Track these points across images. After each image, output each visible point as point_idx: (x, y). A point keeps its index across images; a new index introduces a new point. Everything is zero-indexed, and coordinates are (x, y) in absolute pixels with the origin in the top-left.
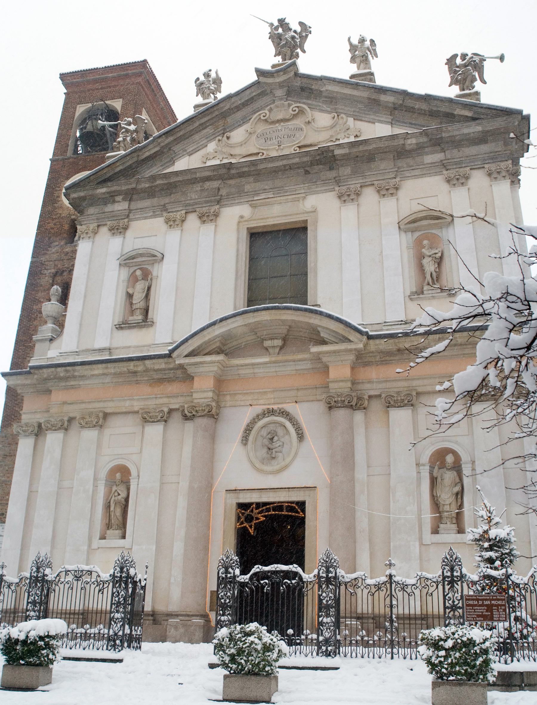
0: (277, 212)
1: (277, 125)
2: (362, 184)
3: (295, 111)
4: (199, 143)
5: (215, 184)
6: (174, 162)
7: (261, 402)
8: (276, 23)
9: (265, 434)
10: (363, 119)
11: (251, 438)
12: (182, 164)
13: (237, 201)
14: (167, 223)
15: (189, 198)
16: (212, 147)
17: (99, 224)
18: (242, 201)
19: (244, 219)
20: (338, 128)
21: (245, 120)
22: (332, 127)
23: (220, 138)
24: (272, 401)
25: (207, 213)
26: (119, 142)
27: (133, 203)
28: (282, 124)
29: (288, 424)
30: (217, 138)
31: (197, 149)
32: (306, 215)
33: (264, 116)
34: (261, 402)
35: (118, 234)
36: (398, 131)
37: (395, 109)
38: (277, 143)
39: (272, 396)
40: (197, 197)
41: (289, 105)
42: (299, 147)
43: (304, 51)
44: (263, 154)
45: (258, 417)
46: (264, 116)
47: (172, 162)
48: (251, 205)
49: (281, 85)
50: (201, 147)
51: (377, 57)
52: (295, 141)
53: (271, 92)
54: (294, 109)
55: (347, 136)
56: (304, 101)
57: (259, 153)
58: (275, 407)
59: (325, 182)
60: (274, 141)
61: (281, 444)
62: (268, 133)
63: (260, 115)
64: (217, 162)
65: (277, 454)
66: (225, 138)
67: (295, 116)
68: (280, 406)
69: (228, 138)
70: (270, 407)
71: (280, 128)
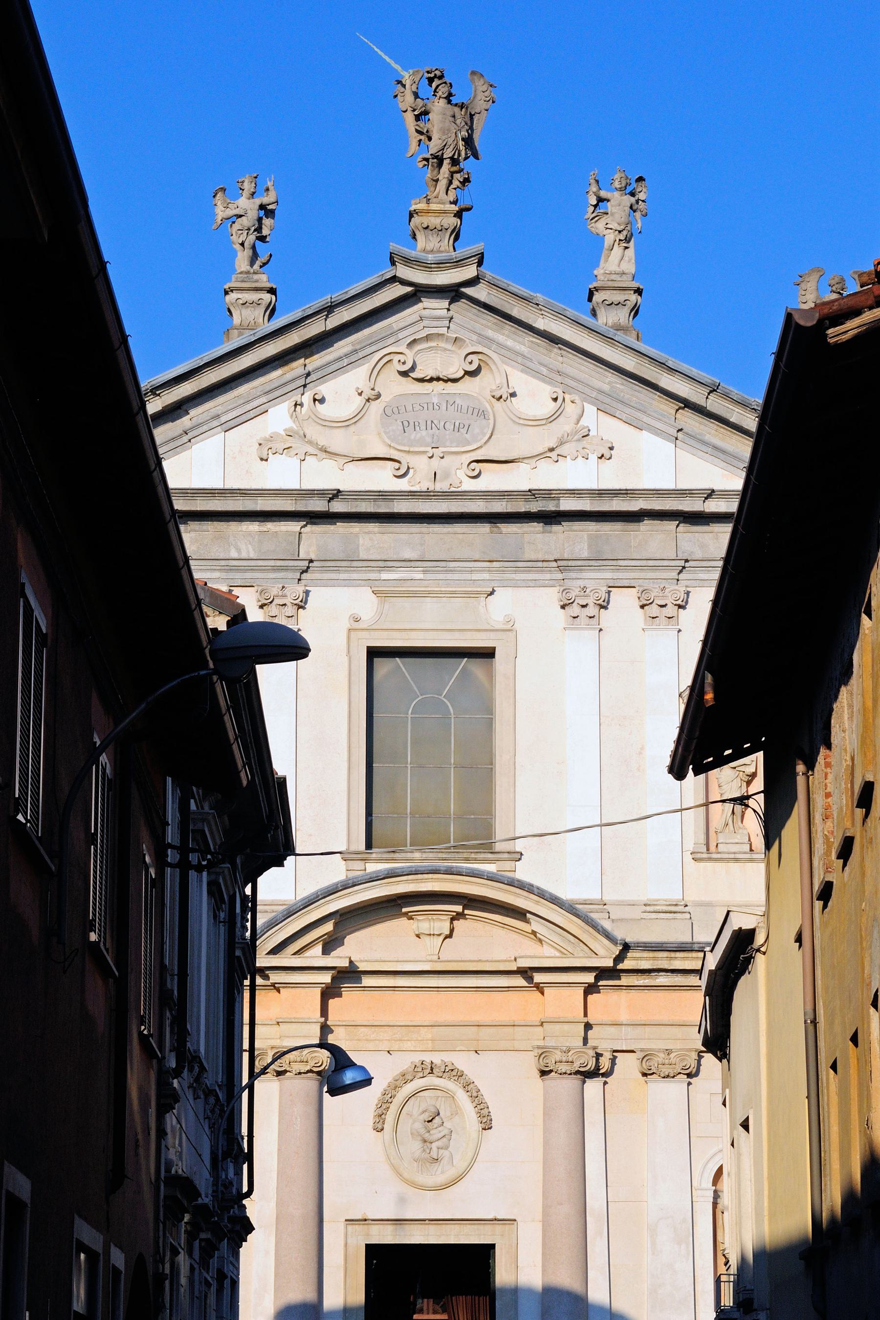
5: (294, 526)
7: (408, 1045)
9: (416, 1113)
11: (390, 1118)
13: (343, 576)
15: (234, 554)
16: (279, 418)
18: (355, 576)
20: (564, 426)
22: (552, 419)
24: (430, 1046)
29: (462, 1096)
31: (244, 418)
32: (492, 635)
34: (408, 1045)
38: (429, 440)
39: (429, 1036)
40: (252, 556)
45: (404, 1078)
52: (469, 443)
58: (437, 1059)
59: (538, 564)
60: (424, 433)
61: (446, 1132)
62: (409, 408)
65: (441, 1152)
66: (307, 399)
68: (448, 1057)
70: (428, 1058)
71: (435, 400)
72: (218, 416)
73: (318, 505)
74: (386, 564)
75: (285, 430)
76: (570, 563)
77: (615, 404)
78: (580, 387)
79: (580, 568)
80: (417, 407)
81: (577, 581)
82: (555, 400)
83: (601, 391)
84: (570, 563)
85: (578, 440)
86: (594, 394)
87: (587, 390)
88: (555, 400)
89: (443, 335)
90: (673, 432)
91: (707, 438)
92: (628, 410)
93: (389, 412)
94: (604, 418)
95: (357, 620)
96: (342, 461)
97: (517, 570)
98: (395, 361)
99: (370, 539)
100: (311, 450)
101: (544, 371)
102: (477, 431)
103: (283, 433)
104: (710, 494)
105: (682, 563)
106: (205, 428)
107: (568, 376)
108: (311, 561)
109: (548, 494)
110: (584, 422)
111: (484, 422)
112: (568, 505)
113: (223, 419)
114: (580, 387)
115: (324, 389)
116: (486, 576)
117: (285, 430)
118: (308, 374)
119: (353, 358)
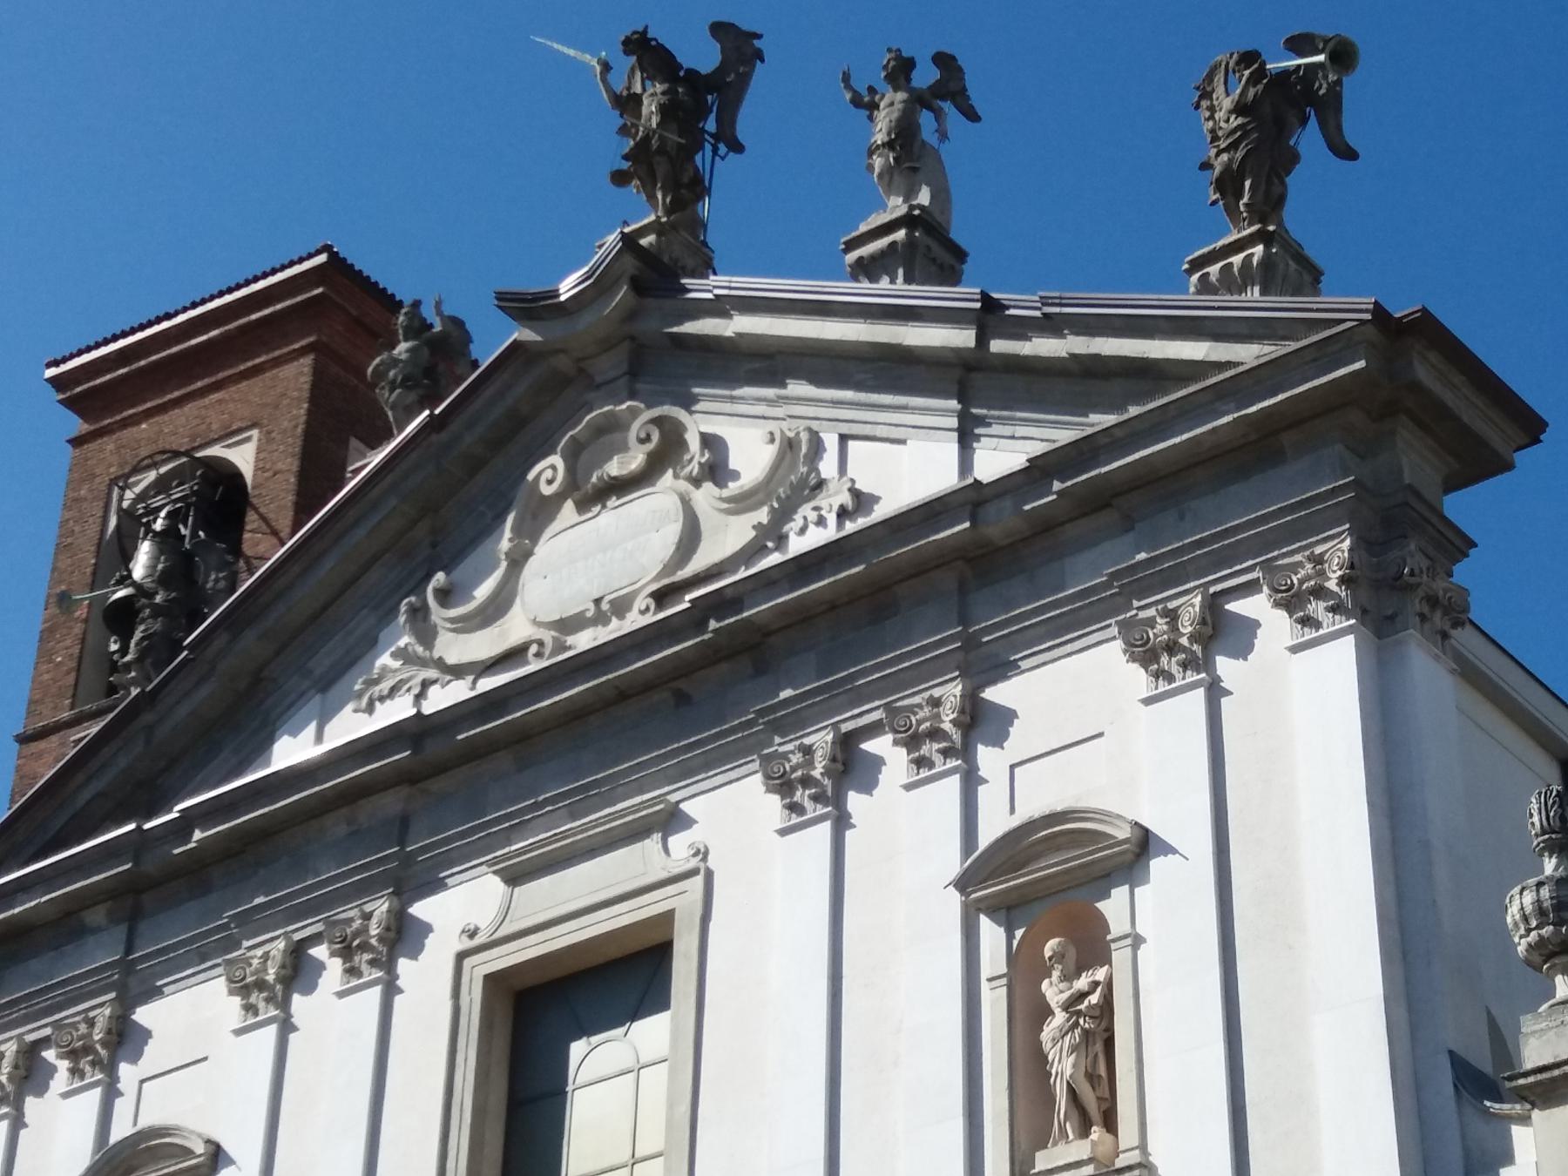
0: (578, 901)
5: (390, 803)
10: (880, 431)
19: (480, 940)
25: (356, 934)
30: (403, 608)
49: (607, 345)
54: (643, 435)
95: (472, 934)
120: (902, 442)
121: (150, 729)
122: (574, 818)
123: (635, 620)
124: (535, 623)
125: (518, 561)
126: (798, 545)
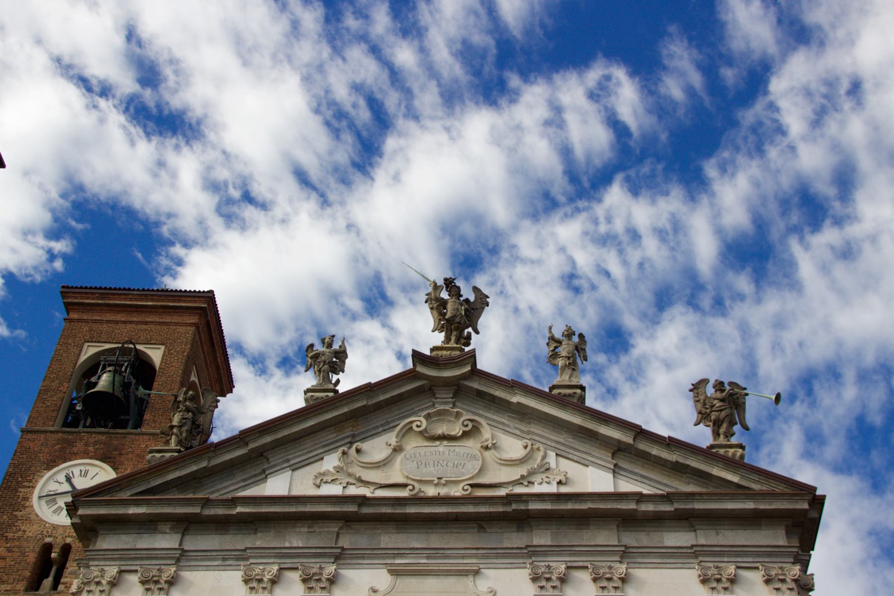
1: (438, 443)
2: (569, 564)
3: (467, 426)
4: (310, 452)
6: (266, 477)
8: (441, 282)
10: (570, 456)
12: (277, 485)
13: (366, 562)
14: (246, 582)
15: (287, 545)
16: (331, 462)
17: (123, 568)
18: (376, 561)
21: (387, 428)
22: (522, 461)
23: (345, 448)
25: (314, 574)
26: (172, 427)
27: (187, 538)
28: (445, 443)
30: (340, 450)
31: (307, 462)
33: (418, 426)
35: (157, 592)
36: (627, 486)
37: (619, 450)
40: (301, 545)
41: (458, 415)
42: (472, 486)
43: (477, 332)
44: (414, 488)
46: (418, 426)
47: (263, 476)
48: (390, 571)
50: (312, 460)
51: (586, 360)
52: (464, 475)
53: (430, 389)
54: (465, 423)
55: (547, 480)
56: (481, 412)
57: (404, 486)
60: (432, 469)
63: (412, 422)
64: (335, 490)
66: (353, 451)
67: (466, 435)
69: (358, 451)
72: (288, 461)
73: (352, 508)
74: (399, 552)
75: (334, 467)
76: (538, 549)
77: (568, 450)
78: (543, 441)
79: (545, 554)
80: (428, 454)
81: (541, 564)
82: (526, 447)
83: (558, 442)
84: (538, 549)
85: (543, 472)
86: (553, 444)
87: (549, 443)
88: (526, 447)
89: (448, 410)
90: (612, 466)
91: (636, 470)
92: (577, 454)
93: (408, 456)
94: (561, 460)
96: (372, 488)
97: (496, 558)
98: (414, 425)
99: (389, 539)
100: (352, 481)
101: (518, 432)
102: (470, 467)
103: (332, 470)
104: (640, 497)
105: (623, 549)
106: (278, 468)
107: (534, 434)
108: (343, 549)
109: (519, 498)
110: (547, 460)
111: (475, 462)
112: (534, 506)
113: (292, 462)
114: (543, 441)
115: (364, 446)
116: (475, 561)
117: (334, 467)
118: (354, 436)
119: (386, 427)
120: (587, 466)
121: (210, 459)
122: (428, 558)
123: (456, 491)
124: (407, 477)
125: (397, 450)
126: (536, 489)
